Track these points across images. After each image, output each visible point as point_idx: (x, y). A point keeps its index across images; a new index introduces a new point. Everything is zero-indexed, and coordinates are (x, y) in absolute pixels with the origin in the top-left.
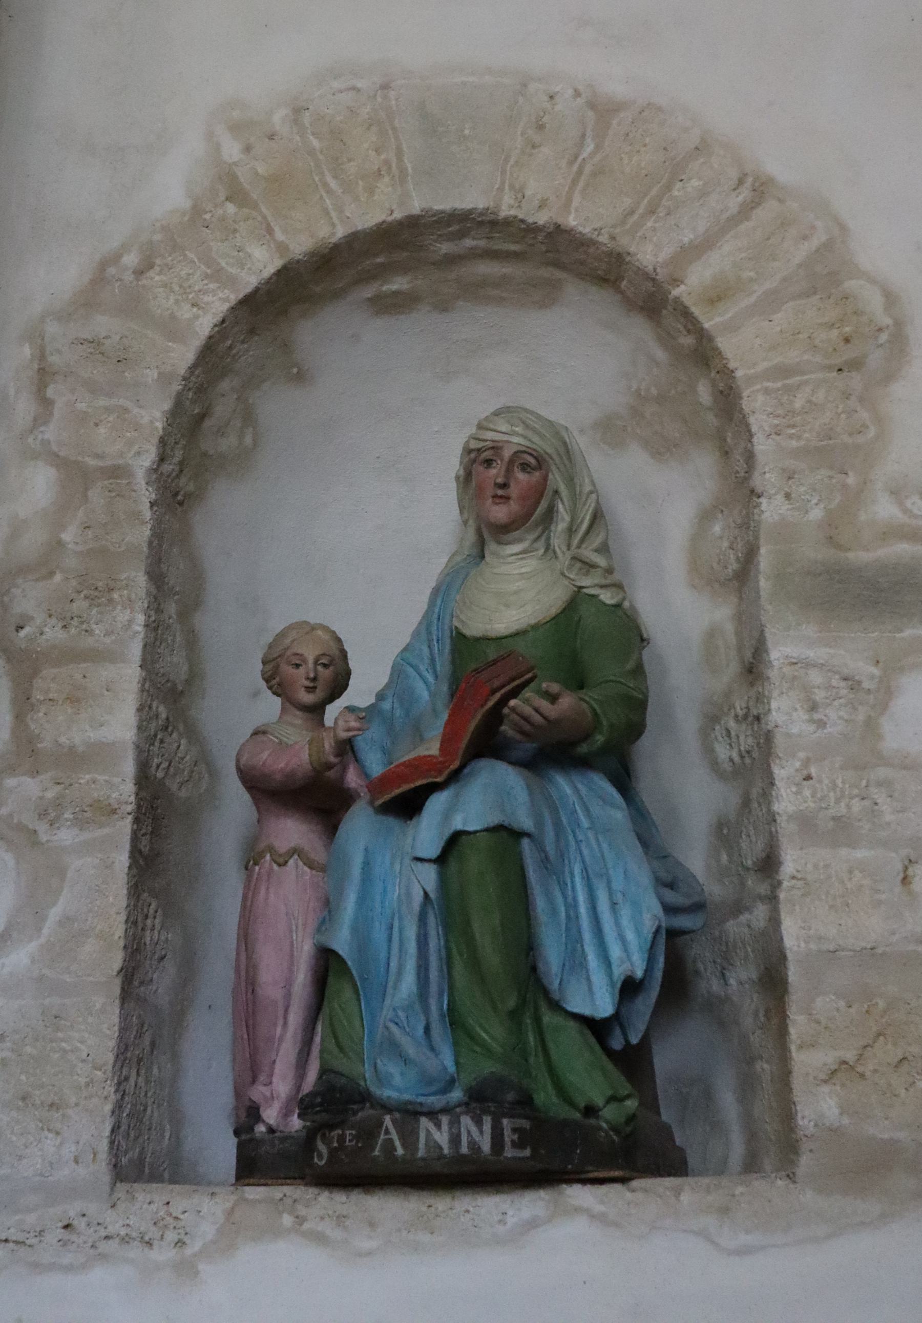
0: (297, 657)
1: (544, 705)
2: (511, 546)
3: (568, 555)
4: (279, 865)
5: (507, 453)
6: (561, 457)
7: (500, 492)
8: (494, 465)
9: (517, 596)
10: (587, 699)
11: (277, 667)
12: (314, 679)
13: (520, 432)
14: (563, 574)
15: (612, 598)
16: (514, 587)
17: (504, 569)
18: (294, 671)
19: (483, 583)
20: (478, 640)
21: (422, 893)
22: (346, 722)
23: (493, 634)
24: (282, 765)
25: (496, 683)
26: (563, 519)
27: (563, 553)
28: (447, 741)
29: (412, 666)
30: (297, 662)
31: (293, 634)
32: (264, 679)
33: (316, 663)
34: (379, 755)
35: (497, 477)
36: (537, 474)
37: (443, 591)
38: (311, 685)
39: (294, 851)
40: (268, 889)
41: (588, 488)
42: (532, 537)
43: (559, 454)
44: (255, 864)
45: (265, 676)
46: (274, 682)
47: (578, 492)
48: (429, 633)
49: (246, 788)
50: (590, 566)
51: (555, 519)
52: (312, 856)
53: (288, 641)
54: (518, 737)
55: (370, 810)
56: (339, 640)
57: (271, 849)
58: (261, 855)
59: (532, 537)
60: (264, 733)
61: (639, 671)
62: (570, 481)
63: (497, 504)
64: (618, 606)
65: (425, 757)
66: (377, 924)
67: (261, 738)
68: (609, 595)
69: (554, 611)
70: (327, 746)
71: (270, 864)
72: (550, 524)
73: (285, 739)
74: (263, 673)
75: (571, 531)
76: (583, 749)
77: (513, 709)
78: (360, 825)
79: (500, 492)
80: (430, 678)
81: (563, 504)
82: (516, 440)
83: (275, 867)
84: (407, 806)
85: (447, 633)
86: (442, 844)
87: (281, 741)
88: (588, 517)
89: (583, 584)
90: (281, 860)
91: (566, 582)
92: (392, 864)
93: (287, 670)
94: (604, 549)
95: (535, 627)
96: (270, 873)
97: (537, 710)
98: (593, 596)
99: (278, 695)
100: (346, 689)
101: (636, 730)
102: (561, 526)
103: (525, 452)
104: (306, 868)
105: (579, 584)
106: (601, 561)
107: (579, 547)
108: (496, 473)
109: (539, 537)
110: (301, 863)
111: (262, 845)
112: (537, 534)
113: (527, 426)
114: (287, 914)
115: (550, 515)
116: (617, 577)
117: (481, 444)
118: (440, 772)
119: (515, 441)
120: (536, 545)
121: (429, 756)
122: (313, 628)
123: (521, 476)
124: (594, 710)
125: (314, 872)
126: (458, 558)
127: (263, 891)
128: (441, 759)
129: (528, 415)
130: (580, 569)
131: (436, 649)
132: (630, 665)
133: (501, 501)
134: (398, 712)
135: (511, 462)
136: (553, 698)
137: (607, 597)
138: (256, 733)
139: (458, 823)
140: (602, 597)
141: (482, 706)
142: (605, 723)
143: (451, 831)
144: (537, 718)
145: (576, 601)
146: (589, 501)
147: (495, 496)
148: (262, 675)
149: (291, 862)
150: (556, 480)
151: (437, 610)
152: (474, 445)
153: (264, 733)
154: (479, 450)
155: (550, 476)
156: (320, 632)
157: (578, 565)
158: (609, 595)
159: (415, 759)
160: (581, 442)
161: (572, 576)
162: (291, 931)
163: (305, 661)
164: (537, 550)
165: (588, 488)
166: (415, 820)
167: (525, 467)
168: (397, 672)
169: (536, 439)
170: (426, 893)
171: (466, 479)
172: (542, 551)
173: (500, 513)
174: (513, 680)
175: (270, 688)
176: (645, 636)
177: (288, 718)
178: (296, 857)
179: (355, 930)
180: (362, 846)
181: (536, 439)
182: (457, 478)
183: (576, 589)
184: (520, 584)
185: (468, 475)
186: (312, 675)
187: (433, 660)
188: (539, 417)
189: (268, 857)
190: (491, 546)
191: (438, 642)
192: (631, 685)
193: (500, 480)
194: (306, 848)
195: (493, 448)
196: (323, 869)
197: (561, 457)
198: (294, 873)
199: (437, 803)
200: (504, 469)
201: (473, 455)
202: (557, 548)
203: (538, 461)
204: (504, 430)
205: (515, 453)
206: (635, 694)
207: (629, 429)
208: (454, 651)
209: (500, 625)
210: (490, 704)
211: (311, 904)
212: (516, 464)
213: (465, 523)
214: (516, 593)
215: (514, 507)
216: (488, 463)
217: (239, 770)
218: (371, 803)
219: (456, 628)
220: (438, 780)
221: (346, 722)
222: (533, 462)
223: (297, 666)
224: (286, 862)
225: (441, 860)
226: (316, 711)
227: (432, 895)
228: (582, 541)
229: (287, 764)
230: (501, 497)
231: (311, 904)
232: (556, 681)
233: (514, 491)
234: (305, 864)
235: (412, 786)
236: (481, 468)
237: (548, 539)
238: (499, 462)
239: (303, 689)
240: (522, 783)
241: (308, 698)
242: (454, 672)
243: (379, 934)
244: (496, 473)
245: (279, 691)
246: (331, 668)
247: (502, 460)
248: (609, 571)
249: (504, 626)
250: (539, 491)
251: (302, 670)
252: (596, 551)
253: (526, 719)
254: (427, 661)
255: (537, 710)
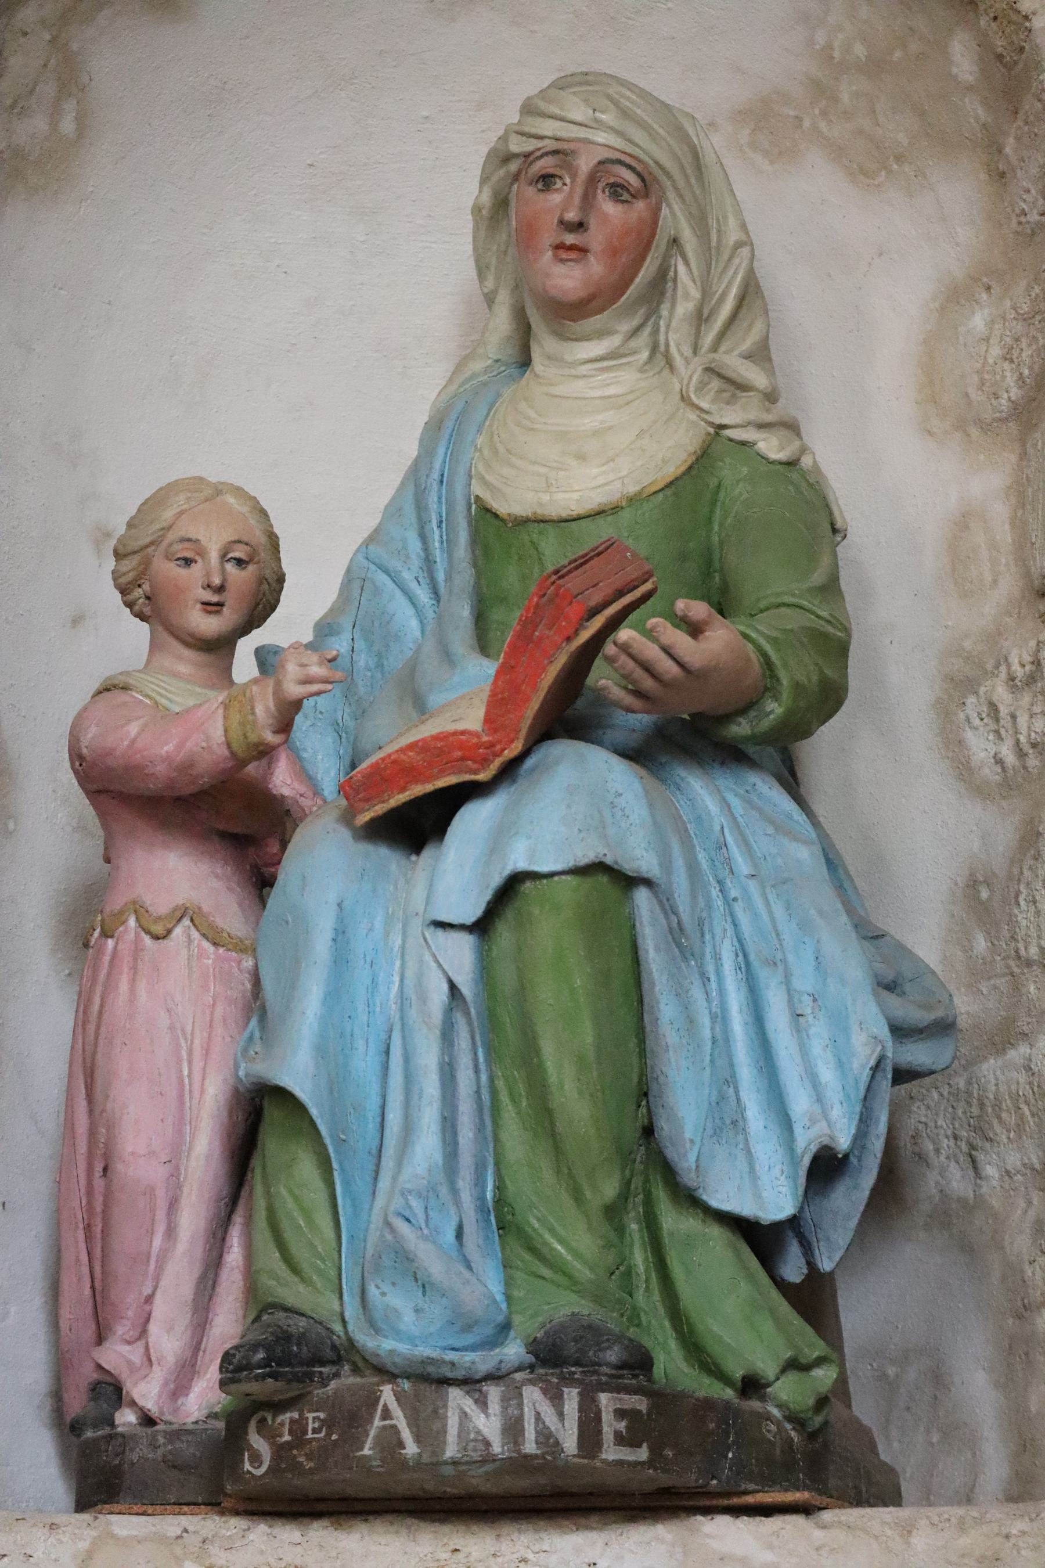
0: (186, 545)
1: (680, 640)
2: (585, 344)
3: (697, 365)
4: (156, 937)
5: (585, 164)
6: (686, 177)
7: (570, 239)
8: (559, 184)
9: (596, 439)
10: (754, 635)
11: (147, 563)
12: (220, 589)
13: (611, 124)
14: (684, 399)
15: (782, 448)
16: (590, 423)
17: (578, 387)
18: (183, 572)
19: (532, 414)
20: (523, 522)
21: (445, 987)
22: (303, 665)
23: (553, 512)
24: (169, 748)
25: (596, 597)
26: (687, 296)
27: (687, 361)
28: (501, 701)
29: (387, 572)
30: (188, 554)
31: (180, 501)
32: (117, 586)
33: (224, 557)
34: (330, 739)
35: (565, 209)
36: (640, 205)
37: (447, 427)
38: (215, 599)
39: (181, 913)
40: (133, 981)
41: (733, 235)
42: (625, 327)
43: (682, 168)
44: (106, 934)
45: (123, 580)
46: (138, 593)
47: (714, 244)
48: (420, 507)
49: (88, 793)
50: (738, 386)
51: (668, 295)
52: (220, 922)
53: (168, 515)
54: (629, 700)
55: (345, 834)
56: (264, 513)
57: (138, 909)
58: (120, 918)
59: (625, 327)
60: (125, 688)
61: (831, 588)
62: (701, 221)
63: (562, 261)
64: (791, 464)
65: (455, 733)
66: (360, 1044)
67: (121, 697)
68: (774, 441)
69: (671, 471)
70: (259, 710)
71: (137, 935)
72: (659, 303)
73: (164, 701)
74: (116, 575)
75: (701, 318)
76: (741, 729)
77: (625, 648)
78: (326, 865)
79: (570, 239)
80: (423, 595)
81: (687, 263)
82: (601, 137)
83: (147, 940)
84: (416, 826)
85: (461, 508)
86: (488, 895)
87: (156, 703)
88: (734, 291)
89: (725, 421)
90: (159, 929)
91: (692, 416)
92: (387, 934)
93: (166, 569)
94: (761, 355)
95: (633, 500)
96: (137, 949)
97: (667, 651)
98: (743, 443)
99: (143, 617)
100: (273, 609)
101: (827, 699)
102: (683, 306)
103: (620, 162)
104: (206, 944)
105: (718, 421)
106: (758, 378)
107: (714, 348)
108: (560, 201)
109: (636, 331)
110: (195, 934)
111: (117, 901)
112: (636, 322)
113: (625, 114)
114: (172, 1028)
115: (661, 285)
116: (783, 409)
117: (530, 145)
118: (485, 762)
119: (601, 140)
120: (633, 344)
121: (463, 733)
122: (219, 490)
123: (609, 208)
124: (764, 655)
125: (221, 950)
126: (477, 366)
127: (124, 986)
128: (485, 739)
129: (624, 91)
130: (721, 391)
131: (437, 537)
132: (818, 578)
133: (573, 255)
134: (363, 660)
135: (592, 180)
136: (695, 630)
137: (771, 446)
138: (107, 689)
139: (518, 860)
140: (762, 446)
141: (569, 639)
142: (785, 682)
143: (507, 872)
144: (668, 667)
145: (712, 450)
146: (736, 261)
147: (559, 247)
148: (115, 579)
149: (178, 931)
150: (675, 218)
151: (437, 466)
152: (517, 145)
153: (125, 688)
154: (527, 156)
155: (665, 211)
156: (231, 500)
157: (716, 384)
158: (774, 441)
159: (436, 738)
160: (716, 145)
161: (705, 405)
162: (179, 1062)
163: (202, 553)
164: (635, 352)
165: (733, 235)
166: (427, 853)
167: (617, 190)
168: (354, 583)
169: (639, 136)
170: (453, 987)
171: (495, 213)
172: (645, 355)
173: (568, 279)
174: (620, 593)
175: (129, 605)
176: (839, 525)
177: (166, 661)
178: (186, 922)
179: (321, 1051)
180: (332, 897)
181: (639, 136)
182: (477, 210)
183: (712, 430)
184: (609, 417)
185: (501, 204)
186: (217, 581)
187: (429, 562)
188: (643, 94)
189: (132, 922)
190: (544, 344)
191: (440, 527)
192: (824, 614)
193: (572, 216)
194: (206, 908)
195: (555, 152)
196: (242, 948)
197: (686, 177)
198: (184, 952)
199: (473, 820)
200: (579, 191)
201: (514, 166)
202: (673, 350)
203: (643, 180)
204: (579, 117)
205: (601, 163)
206: (830, 629)
207: (807, 123)
208: (476, 539)
209: (567, 495)
210: (585, 636)
211: (219, 1011)
212: (601, 185)
213: (490, 299)
214: (596, 433)
215: (596, 267)
216: (546, 180)
217: (77, 758)
218: (347, 818)
219: (477, 496)
220: (482, 777)
221: (303, 665)
222: (631, 182)
223: (188, 562)
224: (169, 932)
225: (481, 928)
226: (220, 648)
227: (467, 990)
228: (721, 336)
229: (181, 745)
230: (571, 248)
231: (219, 1011)
232: (702, 598)
233: (596, 238)
234: (204, 935)
235: (429, 788)
236: (530, 191)
237: (656, 331)
238: (568, 181)
239: (199, 606)
240: (637, 785)
241: (209, 625)
242: (477, 584)
243: (364, 1063)
244: (560, 201)
245: (147, 611)
246: (251, 568)
247: (574, 176)
248: (771, 397)
249: (576, 496)
250: (644, 237)
251: (196, 569)
252: (748, 356)
253: (648, 668)
254: (416, 562)
255: (667, 651)
